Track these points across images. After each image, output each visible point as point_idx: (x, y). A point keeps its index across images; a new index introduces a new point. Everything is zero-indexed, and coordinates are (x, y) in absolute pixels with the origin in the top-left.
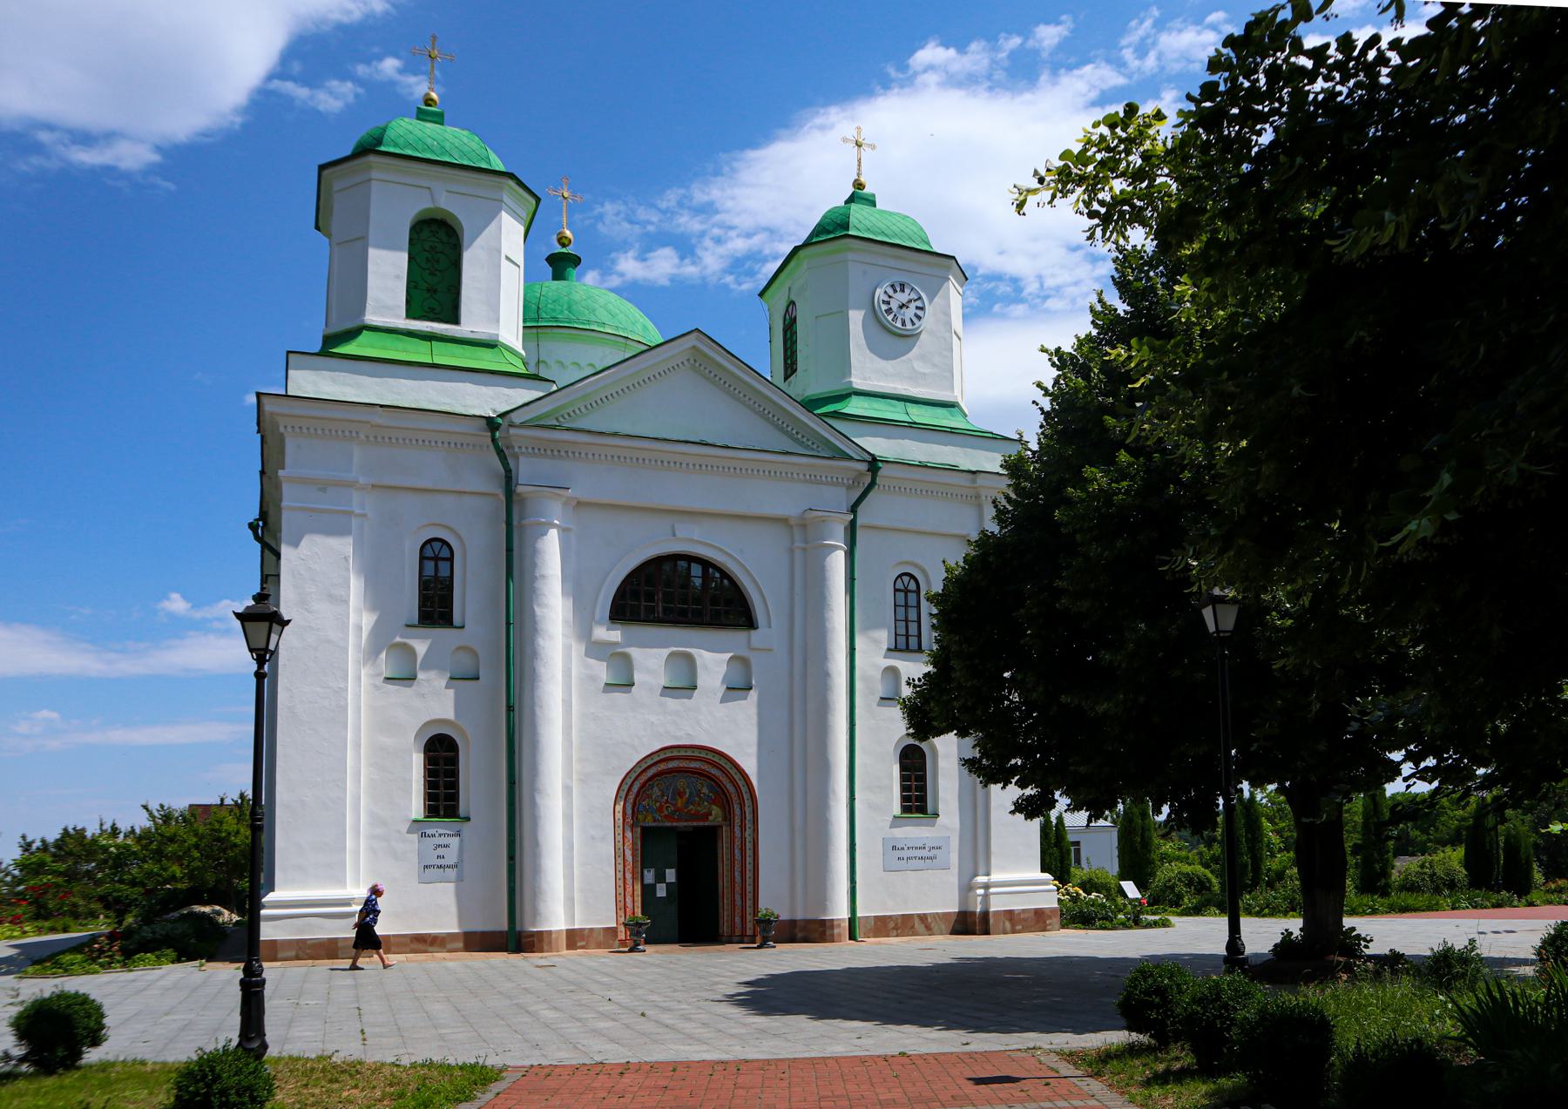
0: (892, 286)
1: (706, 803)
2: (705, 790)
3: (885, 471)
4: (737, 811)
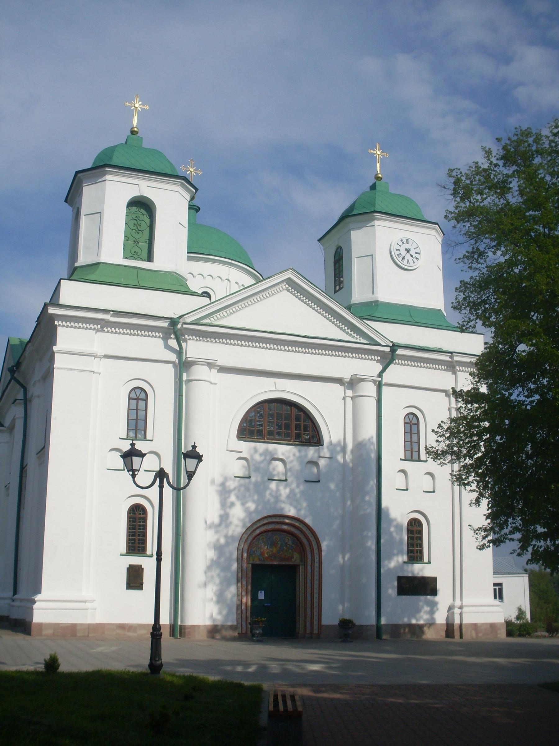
0: (401, 240)
1: (290, 551)
2: (290, 543)
3: (400, 352)
4: (309, 556)
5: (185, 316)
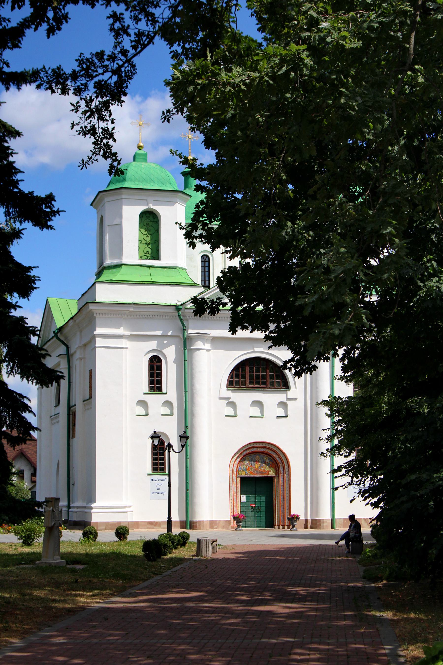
2: (268, 461)
5: (186, 304)
